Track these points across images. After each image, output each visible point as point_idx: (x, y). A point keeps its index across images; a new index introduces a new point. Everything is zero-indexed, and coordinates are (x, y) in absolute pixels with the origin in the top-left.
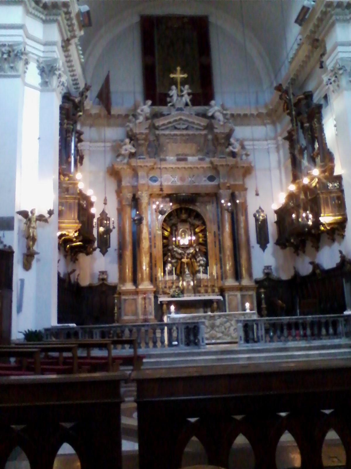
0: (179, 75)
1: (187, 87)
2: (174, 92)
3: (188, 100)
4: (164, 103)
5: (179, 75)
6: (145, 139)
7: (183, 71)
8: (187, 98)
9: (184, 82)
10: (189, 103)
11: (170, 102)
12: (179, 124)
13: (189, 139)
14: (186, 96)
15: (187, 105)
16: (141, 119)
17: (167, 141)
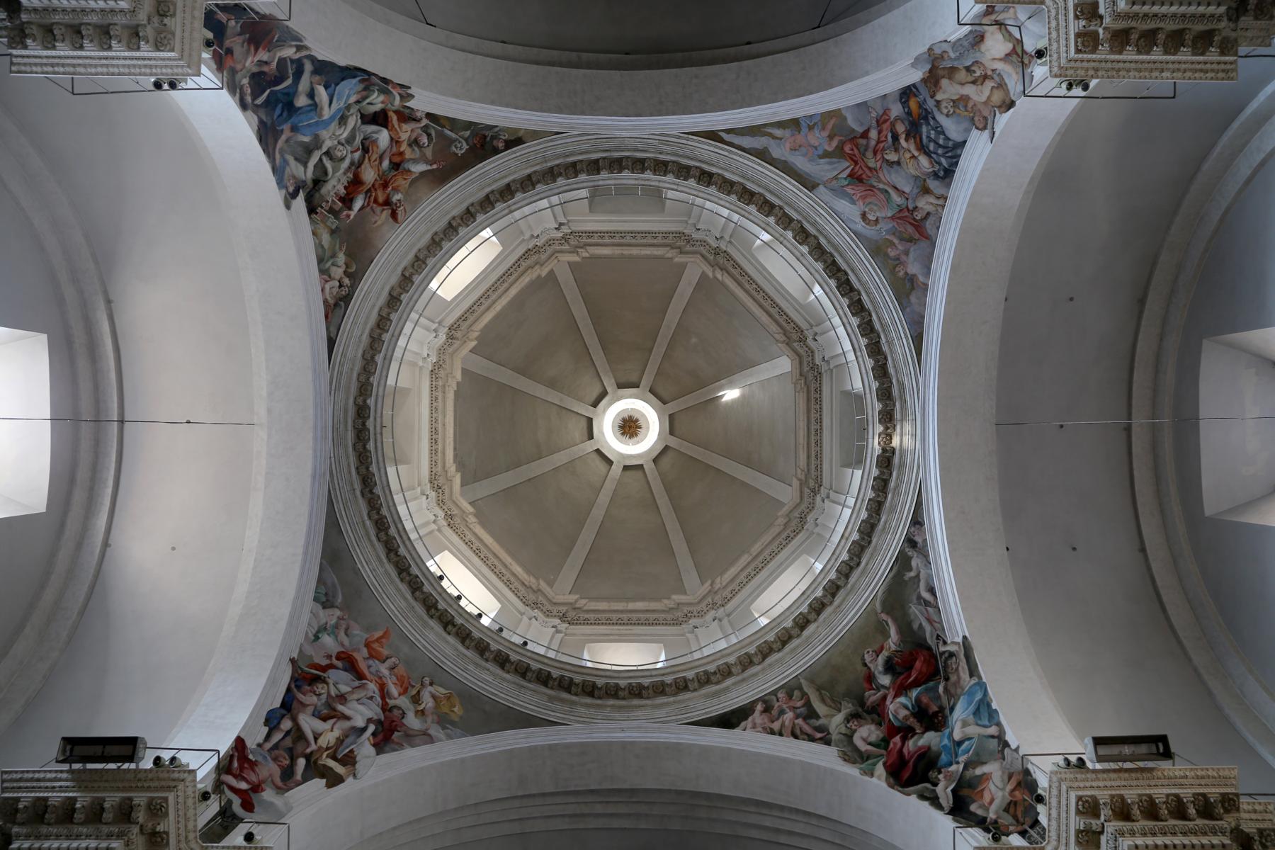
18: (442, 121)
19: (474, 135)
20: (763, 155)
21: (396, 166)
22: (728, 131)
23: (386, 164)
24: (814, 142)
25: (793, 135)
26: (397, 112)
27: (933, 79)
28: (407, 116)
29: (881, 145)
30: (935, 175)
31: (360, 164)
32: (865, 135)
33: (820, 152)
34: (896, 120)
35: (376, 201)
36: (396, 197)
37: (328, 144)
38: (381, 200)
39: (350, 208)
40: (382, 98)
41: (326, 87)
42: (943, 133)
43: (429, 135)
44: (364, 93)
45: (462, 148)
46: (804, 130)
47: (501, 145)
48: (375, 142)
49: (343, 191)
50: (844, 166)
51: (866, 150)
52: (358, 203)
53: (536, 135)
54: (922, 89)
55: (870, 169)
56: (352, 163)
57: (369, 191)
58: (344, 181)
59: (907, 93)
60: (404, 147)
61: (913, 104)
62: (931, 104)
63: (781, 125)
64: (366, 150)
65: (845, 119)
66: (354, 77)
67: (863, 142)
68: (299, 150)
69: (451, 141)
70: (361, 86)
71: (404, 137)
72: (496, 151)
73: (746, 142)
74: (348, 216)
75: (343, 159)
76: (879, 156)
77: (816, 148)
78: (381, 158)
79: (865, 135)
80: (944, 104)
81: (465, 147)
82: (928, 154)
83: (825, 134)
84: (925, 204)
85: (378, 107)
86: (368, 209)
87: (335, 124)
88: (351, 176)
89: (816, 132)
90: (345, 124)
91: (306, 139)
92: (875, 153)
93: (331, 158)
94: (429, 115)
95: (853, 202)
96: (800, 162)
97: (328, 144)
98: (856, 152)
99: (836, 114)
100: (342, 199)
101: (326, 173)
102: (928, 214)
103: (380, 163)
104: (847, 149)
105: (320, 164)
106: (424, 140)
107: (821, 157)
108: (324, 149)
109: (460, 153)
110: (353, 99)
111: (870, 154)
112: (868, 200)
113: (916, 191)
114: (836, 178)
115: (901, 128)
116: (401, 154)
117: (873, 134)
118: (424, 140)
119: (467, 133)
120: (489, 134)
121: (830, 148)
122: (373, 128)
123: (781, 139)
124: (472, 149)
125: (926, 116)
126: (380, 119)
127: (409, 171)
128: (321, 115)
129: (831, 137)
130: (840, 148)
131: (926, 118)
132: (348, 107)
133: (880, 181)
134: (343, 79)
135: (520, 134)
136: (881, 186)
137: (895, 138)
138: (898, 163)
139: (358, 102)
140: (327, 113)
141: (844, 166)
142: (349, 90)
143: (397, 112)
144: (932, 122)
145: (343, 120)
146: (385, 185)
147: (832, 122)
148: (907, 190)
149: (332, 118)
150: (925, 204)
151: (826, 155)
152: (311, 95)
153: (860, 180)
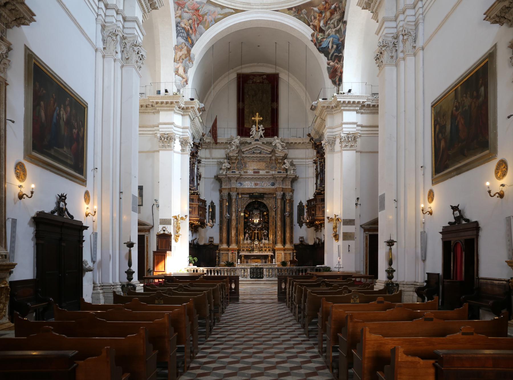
0: (257, 118)
1: (262, 126)
2: (254, 129)
3: (262, 134)
4: (248, 135)
5: (257, 118)
6: (236, 159)
7: (261, 115)
8: (261, 133)
9: (260, 123)
10: (263, 136)
11: (252, 135)
12: (256, 150)
13: (261, 160)
14: (261, 131)
15: (261, 136)
16: (234, 147)
17: (249, 160)
18: (307, 22)
19: (300, 15)
20: (222, 7)
21: (321, 13)
22: (232, 14)
23: (323, 15)
24: (210, 17)
25: (216, 17)
26: (317, 30)
27: (189, 51)
28: (314, 28)
29: (194, 23)
30: (179, 23)
31: (329, 18)
32: (198, 24)
33: (208, 14)
34: (192, 33)
35: (329, 5)
36: (323, 3)
37: (334, 30)
38: (327, 4)
39: (335, 6)
40: (319, 36)
41: (329, 47)
42: (182, 37)
43: (311, 19)
44: (322, 40)
45: (304, 11)
46: (213, 20)
47: (293, 9)
48: (324, 24)
49: (335, 13)
50: (201, 13)
51: (197, 20)
52: (333, 6)
53: (283, 11)
54: (190, 48)
55: (195, 15)
56: (331, 20)
57: (330, 9)
58: (334, 16)
59: (192, 44)
60: (318, 18)
61: (190, 41)
62: (187, 44)
63: (219, 19)
64: (327, 22)
65: (204, 27)
66: (322, 47)
67: (198, 22)
68: (340, 33)
69: (306, 14)
70: (322, 43)
71: (317, 21)
72: (295, 7)
73: (227, 11)
74: (336, 4)
75: (332, 23)
76: (193, 20)
77: (209, 15)
78: (324, 18)
79: (198, 24)
80: (184, 46)
81: (303, 11)
82: (183, 28)
83: (208, 20)
84: (179, 12)
85: (320, 34)
86: (331, 3)
87: (331, 35)
88: (332, 17)
89: (210, 21)
90: (328, 33)
91: (338, 35)
92: (194, 20)
93: (335, 25)
94: (309, 25)
95: (196, 2)
96: (212, 8)
97: (334, 30)
98: (199, 18)
99: (207, 28)
100: (336, 11)
101: (337, 22)
102: (177, 10)
103: (324, 16)
104: (201, 18)
105: (338, 25)
106: (312, 17)
107: (207, 13)
108: (335, 29)
109: (304, 10)
110: (325, 40)
111: (196, 19)
112: (193, 5)
113: (182, 14)
114: (202, 8)
115: (191, 31)
116: (319, 16)
117: (196, 26)
118: (312, 17)
119: (302, 15)
120: (296, 14)
121: (206, 16)
122: (323, 28)
123: (219, 14)
124: (301, 10)
125: (186, 40)
126: (321, 31)
127: (319, 9)
128: (333, 39)
129: (206, 20)
130: (203, 18)
131: (186, 38)
132: (326, 38)
133: (191, 12)
134: (325, 48)
135: (288, 12)
136: (191, 11)
137: (191, 28)
138: (188, 20)
139: (324, 38)
140: (331, 39)
141: (201, 13)
142: (324, 45)
143: (317, 30)
144: (185, 38)
145: (329, 35)
146: (325, 8)
147: (206, 25)
148: (184, 14)
149: (331, 37)
150: (179, 12)
151: (206, 14)
152: (332, 47)
153: (196, 10)
